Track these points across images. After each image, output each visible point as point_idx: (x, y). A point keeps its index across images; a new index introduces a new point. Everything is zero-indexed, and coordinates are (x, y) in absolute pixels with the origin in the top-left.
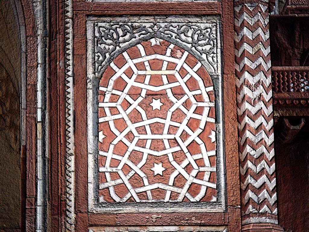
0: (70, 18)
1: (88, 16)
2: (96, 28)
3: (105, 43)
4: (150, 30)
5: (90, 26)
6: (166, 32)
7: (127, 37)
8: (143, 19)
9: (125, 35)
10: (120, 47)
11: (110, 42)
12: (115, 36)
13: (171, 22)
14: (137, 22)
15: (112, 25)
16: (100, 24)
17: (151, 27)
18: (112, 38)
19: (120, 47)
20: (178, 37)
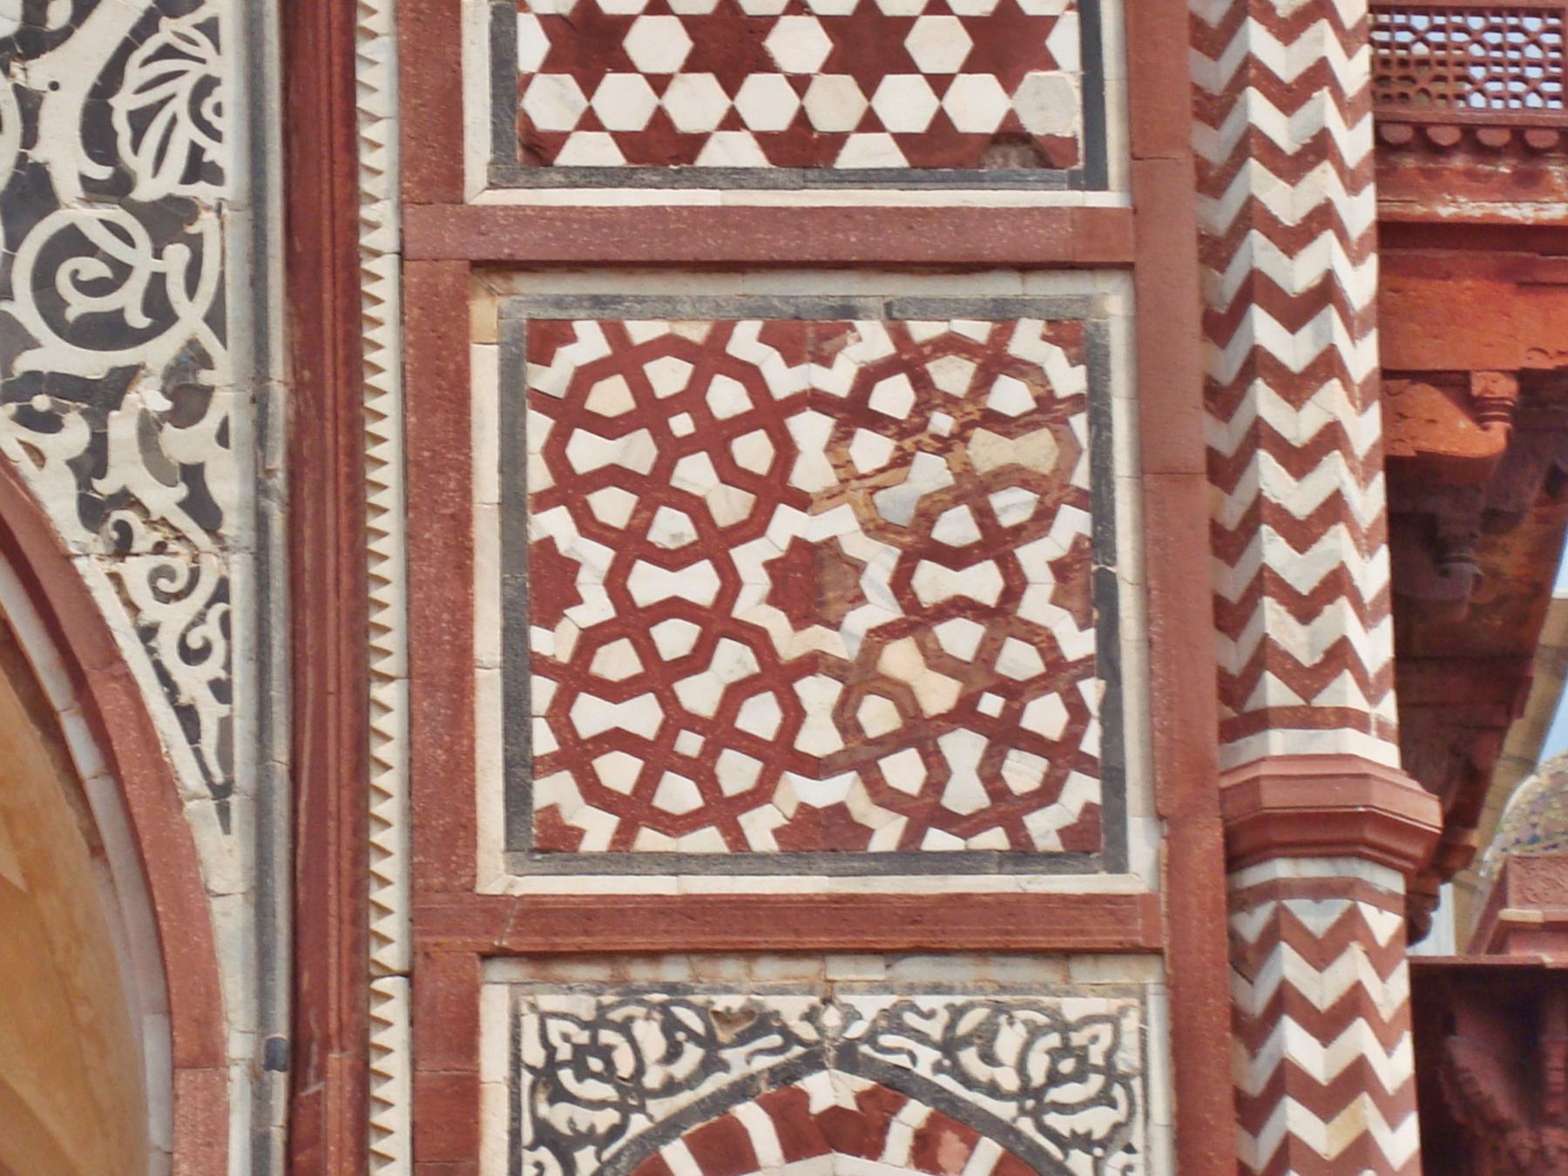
0: (389, 973)
1: (486, 957)
2: (530, 1024)
3: (573, 1099)
4: (807, 1032)
5: (494, 1005)
6: (887, 1040)
7: (681, 1069)
8: (769, 970)
9: (673, 1053)
10: (650, 1118)
11: (607, 1092)
12: (624, 1063)
13: (912, 989)
14: (733, 988)
15: (612, 1007)
16: (550, 1001)
17: (811, 1016)
18: (609, 1074)
19: (650, 1118)
20: (947, 1063)
